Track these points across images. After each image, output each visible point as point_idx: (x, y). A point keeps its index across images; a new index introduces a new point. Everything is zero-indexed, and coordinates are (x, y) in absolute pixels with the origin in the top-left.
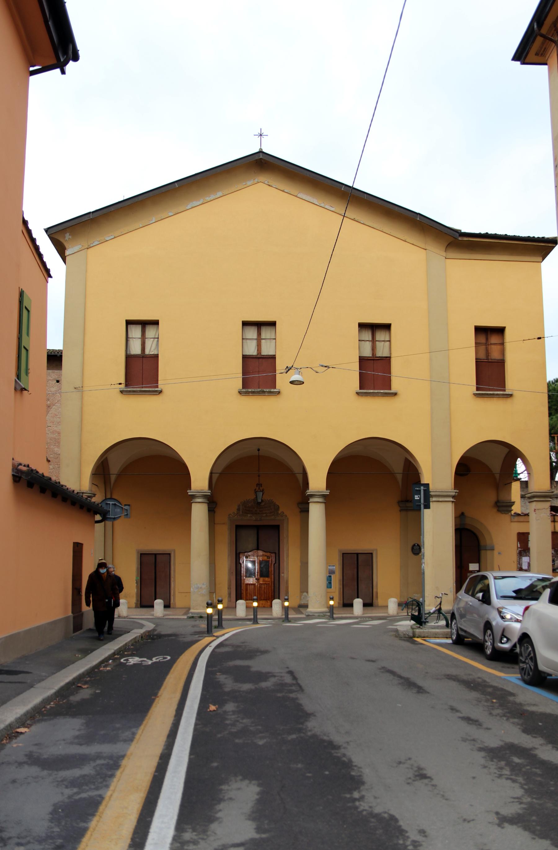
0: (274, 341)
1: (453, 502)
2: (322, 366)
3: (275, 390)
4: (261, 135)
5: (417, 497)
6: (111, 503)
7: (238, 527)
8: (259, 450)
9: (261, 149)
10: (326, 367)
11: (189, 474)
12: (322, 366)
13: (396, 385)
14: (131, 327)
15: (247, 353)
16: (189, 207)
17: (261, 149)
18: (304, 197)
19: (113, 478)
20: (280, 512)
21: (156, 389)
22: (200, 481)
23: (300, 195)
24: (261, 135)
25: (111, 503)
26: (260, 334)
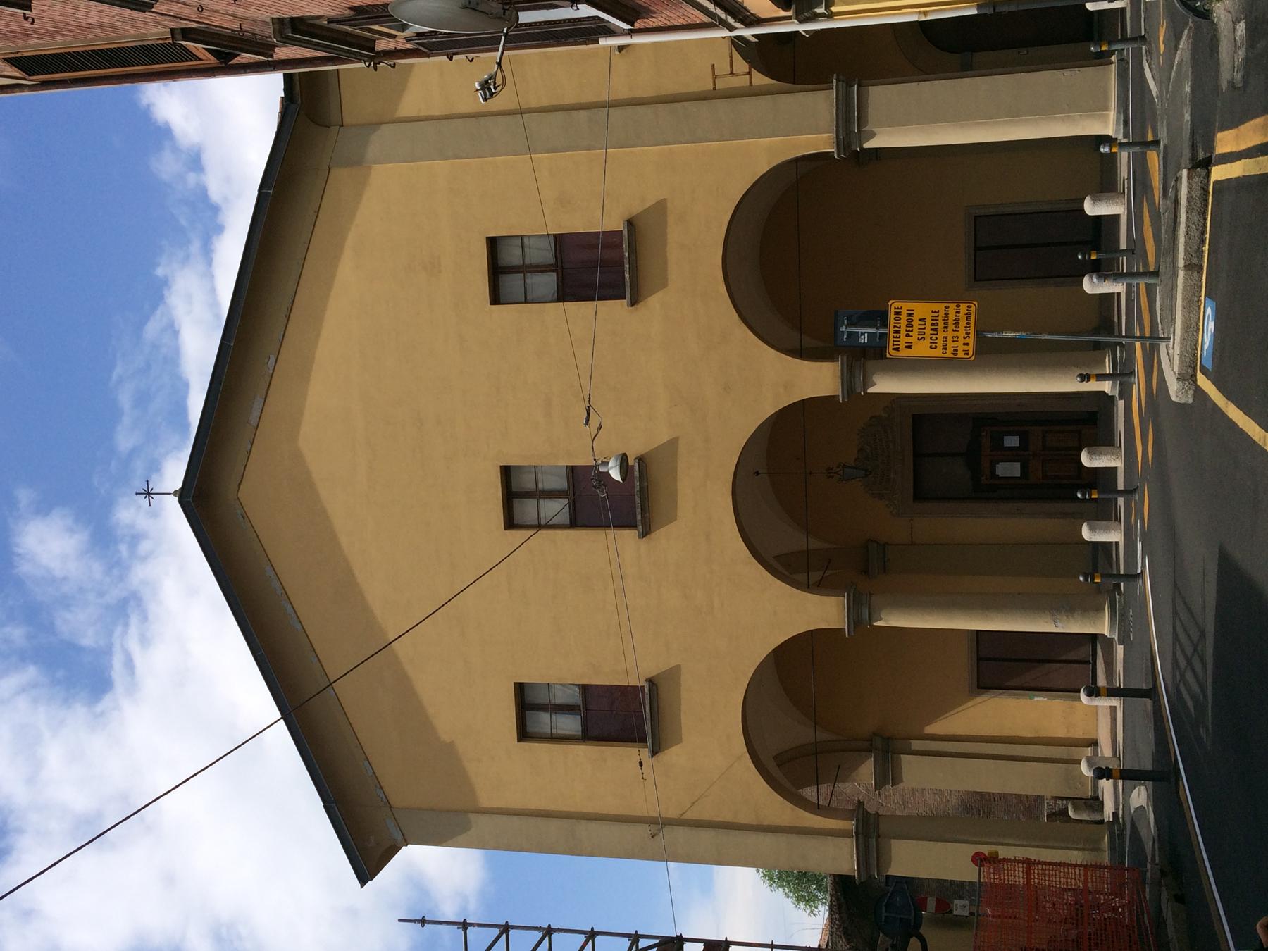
0: (526, 240)
1: (859, 86)
2: (587, 420)
3: (625, 233)
4: (148, 494)
5: (864, 339)
6: (884, 914)
7: (919, 496)
8: (757, 473)
9: (175, 493)
10: (588, 414)
11: (811, 633)
12: (587, 420)
13: (614, 223)
14: (518, 518)
15: (565, 518)
16: (299, 627)
17: (175, 493)
18: (256, 413)
19: (823, 736)
20: (884, 415)
21: (646, 690)
22: (823, 612)
23: (254, 422)
24: (148, 494)
25: (884, 914)
26: (513, 267)
